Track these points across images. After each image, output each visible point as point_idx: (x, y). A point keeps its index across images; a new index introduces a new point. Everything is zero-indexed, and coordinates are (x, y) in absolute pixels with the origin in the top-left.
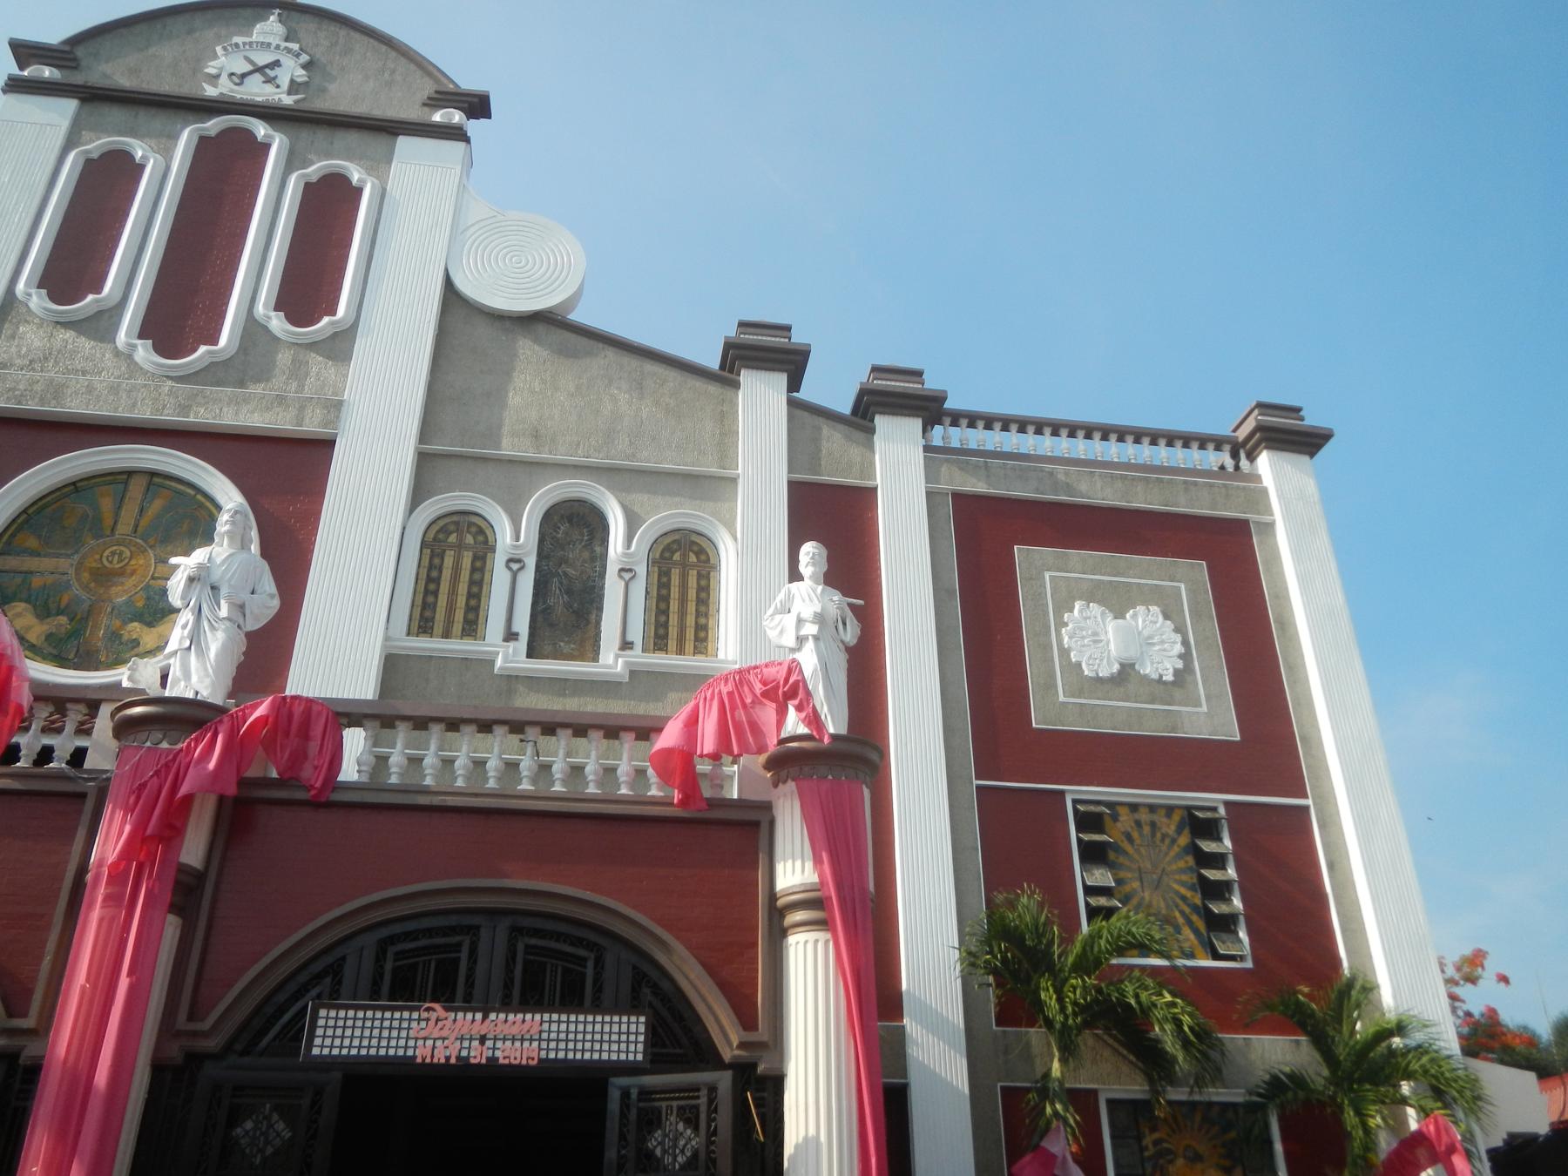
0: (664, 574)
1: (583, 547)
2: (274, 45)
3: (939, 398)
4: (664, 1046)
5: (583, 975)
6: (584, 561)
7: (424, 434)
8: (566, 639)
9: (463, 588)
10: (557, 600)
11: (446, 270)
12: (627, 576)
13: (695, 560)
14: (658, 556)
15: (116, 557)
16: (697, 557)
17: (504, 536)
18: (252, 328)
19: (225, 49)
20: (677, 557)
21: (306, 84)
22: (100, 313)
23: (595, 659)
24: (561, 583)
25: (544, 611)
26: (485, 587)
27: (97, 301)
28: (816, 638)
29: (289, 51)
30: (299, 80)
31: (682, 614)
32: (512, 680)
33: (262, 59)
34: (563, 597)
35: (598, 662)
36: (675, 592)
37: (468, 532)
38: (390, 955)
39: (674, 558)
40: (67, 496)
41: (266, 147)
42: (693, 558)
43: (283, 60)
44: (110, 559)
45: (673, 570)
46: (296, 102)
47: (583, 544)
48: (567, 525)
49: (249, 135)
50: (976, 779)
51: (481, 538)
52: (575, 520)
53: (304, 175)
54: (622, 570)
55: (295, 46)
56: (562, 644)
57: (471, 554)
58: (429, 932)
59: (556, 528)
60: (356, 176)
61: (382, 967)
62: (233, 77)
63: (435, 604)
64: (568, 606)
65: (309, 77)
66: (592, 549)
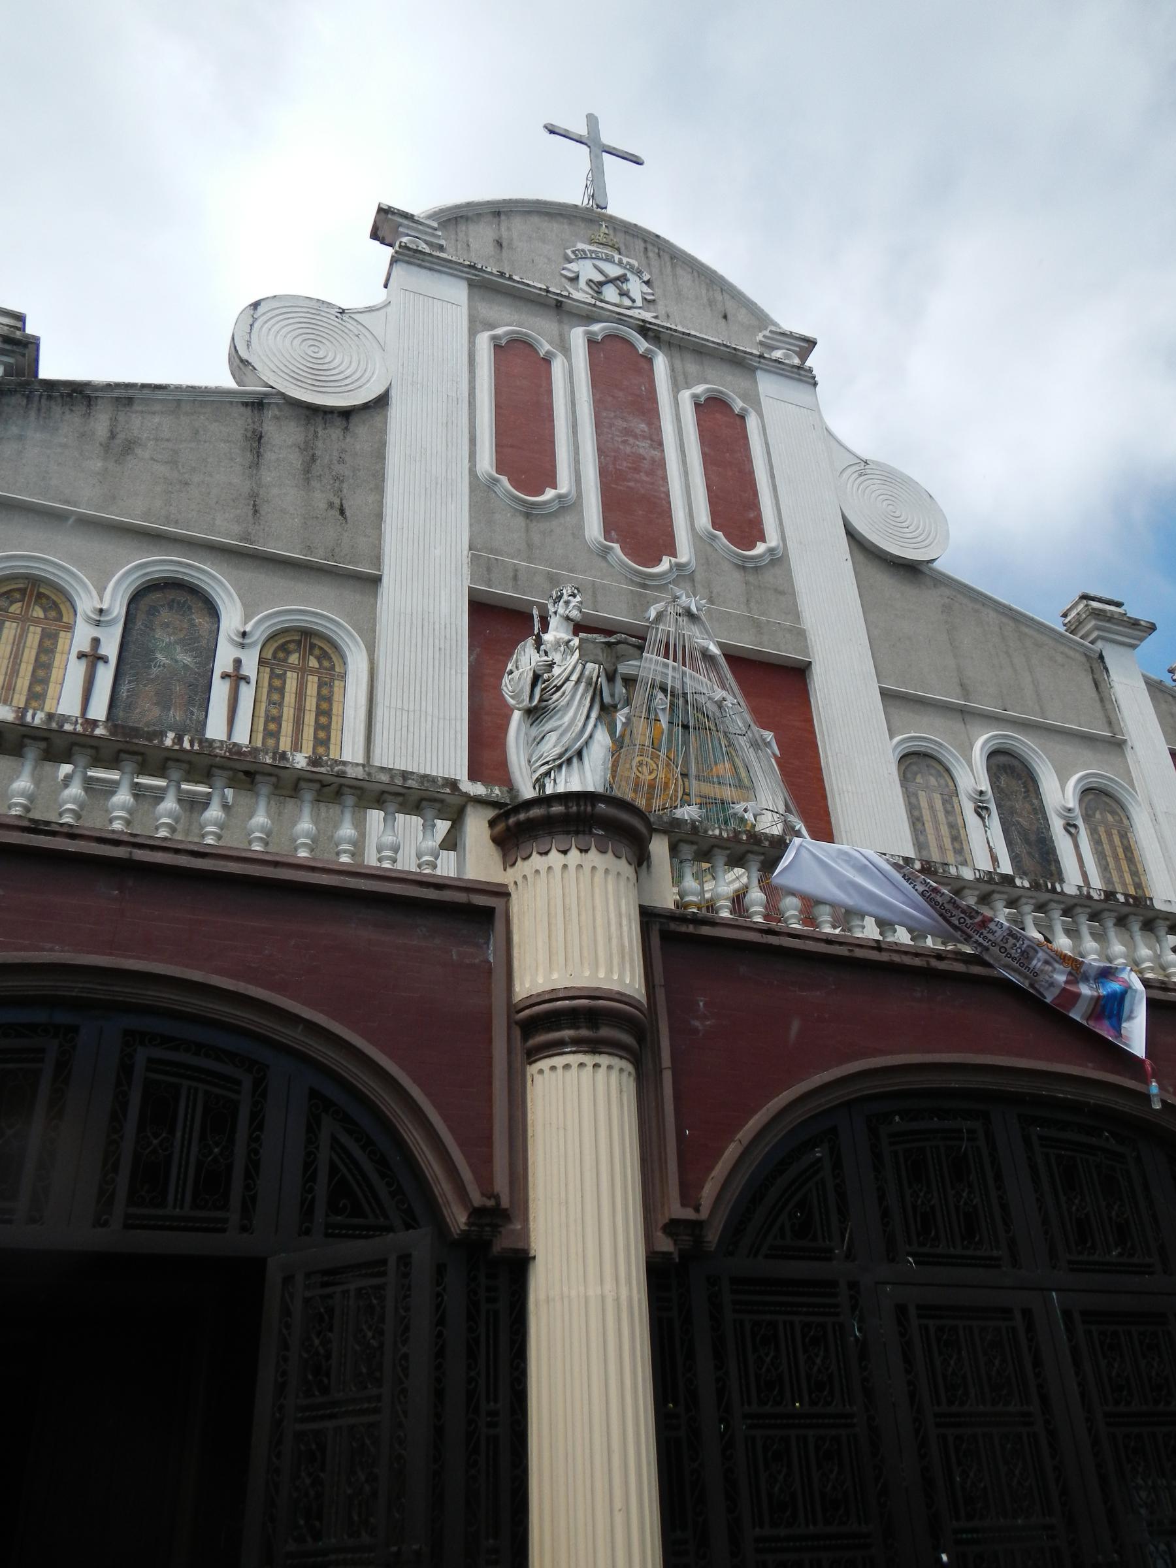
1: (1025, 798)
2: (616, 261)
9: (944, 830)
10: (1022, 849)
13: (1112, 820)
15: (645, 767)
19: (574, 252)
24: (1018, 832)
26: (962, 832)
30: (649, 297)
33: (614, 271)
36: (1106, 847)
37: (931, 775)
41: (649, 360)
43: (629, 275)
45: (1099, 828)
47: (1023, 794)
51: (942, 782)
54: (1068, 824)
59: (998, 778)
62: (591, 284)
64: (1029, 854)
66: (1030, 801)
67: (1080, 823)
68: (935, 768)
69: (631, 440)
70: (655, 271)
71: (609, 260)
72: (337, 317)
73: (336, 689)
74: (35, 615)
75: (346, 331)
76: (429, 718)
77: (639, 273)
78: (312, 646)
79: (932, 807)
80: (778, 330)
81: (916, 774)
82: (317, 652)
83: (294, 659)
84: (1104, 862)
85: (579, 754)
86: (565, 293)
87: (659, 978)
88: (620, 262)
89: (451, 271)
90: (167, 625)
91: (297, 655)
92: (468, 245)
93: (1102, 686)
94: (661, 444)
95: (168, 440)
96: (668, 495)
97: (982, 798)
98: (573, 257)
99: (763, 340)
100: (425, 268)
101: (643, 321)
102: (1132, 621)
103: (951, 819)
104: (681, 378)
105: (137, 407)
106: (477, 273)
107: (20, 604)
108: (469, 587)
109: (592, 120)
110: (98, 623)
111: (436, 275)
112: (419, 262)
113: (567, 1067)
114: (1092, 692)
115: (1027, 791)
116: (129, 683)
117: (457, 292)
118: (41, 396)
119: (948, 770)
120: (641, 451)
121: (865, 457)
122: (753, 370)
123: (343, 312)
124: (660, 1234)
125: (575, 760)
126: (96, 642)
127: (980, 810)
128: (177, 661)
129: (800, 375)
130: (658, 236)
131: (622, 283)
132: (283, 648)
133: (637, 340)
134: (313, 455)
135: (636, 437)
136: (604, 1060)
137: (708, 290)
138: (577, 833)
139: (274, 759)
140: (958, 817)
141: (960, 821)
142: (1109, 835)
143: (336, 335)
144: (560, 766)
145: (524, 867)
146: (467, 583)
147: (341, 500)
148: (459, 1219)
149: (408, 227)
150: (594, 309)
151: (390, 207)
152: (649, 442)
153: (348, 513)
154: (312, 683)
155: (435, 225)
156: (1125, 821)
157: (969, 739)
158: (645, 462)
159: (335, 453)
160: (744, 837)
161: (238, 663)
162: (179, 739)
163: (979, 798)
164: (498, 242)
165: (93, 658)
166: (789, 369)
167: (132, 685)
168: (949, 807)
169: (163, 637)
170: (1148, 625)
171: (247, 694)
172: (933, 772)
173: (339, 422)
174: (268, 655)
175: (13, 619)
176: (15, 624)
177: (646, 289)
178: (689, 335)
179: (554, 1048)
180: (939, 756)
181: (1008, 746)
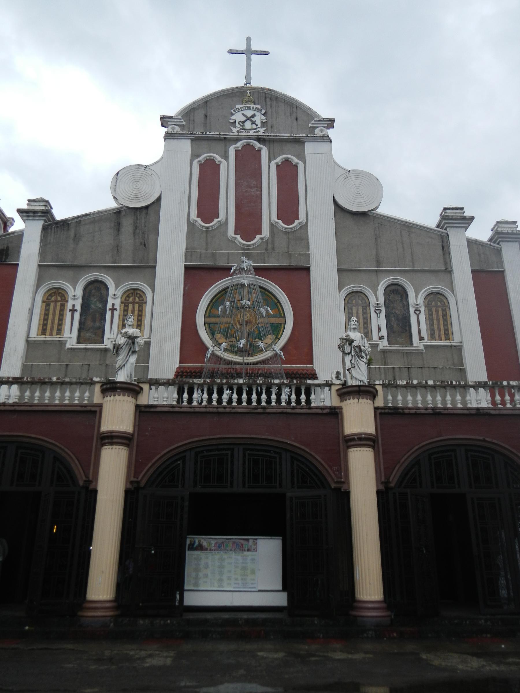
1: (400, 302)
2: (251, 109)
8: (400, 337)
10: (394, 323)
12: (418, 312)
13: (440, 304)
14: (426, 304)
16: (441, 303)
17: (372, 300)
18: (272, 226)
19: (234, 110)
20: (433, 303)
21: (266, 121)
22: (220, 226)
23: (411, 344)
24: (394, 316)
25: (390, 327)
26: (369, 320)
27: (219, 221)
29: (257, 109)
30: (264, 121)
31: (439, 325)
32: (384, 352)
33: (249, 113)
36: (435, 317)
37: (359, 299)
39: (433, 304)
40: (223, 294)
41: (259, 151)
42: (439, 304)
45: (433, 309)
46: (264, 131)
47: (399, 301)
48: (393, 294)
49: (252, 147)
53: (277, 163)
54: (416, 310)
55: (259, 107)
56: (399, 339)
57: (361, 307)
59: (389, 296)
60: (295, 160)
62: (240, 123)
64: (398, 324)
65: (266, 119)
68: (362, 297)
70: (269, 107)
71: (249, 109)
72: (144, 170)
73: (144, 307)
74: (58, 299)
75: (147, 174)
76: (169, 314)
77: (260, 111)
78: (137, 294)
80: (319, 119)
81: (353, 300)
82: (138, 295)
83: (131, 299)
85: (124, 365)
86: (227, 134)
87: (137, 424)
88: (253, 107)
90: (94, 295)
91: (132, 298)
92: (194, 121)
93: (446, 248)
94: (261, 188)
95: (91, 233)
97: (378, 306)
98: (234, 112)
99: (312, 125)
100: (175, 139)
101: (258, 136)
102: (462, 217)
103: (365, 316)
104: (272, 155)
105: (82, 223)
106: (193, 135)
107: (54, 297)
108: (184, 264)
109: (249, 40)
110: (74, 299)
111: (179, 140)
112: (173, 137)
113: (109, 448)
114: (440, 252)
115: (402, 299)
116: (84, 316)
117: (186, 145)
118: (55, 227)
119: (367, 297)
122: (303, 143)
123: (146, 167)
124: (129, 484)
125: (123, 368)
126: (74, 306)
127: (377, 311)
128: (97, 307)
129: (324, 139)
130: (270, 90)
131: (253, 118)
132: (128, 296)
134: (136, 226)
135: (251, 188)
136: (114, 447)
137: (290, 108)
138: (113, 391)
139: (48, 380)
140: (368, 314)
142: (437, 311)
143: (144, 178)
144: (119, 370)
145: (106, 399)
146: (183, 263)
147: (145, 241)
148: (81, 483)
149: (171, 121)
150: (238, 136)
151: (164, 116)
152: (256, 188)
153: (147, 246)
154: (137, 306)
155: (180, 117)
156: (446, 304)
157: (378, 283)
159: (143, 224)
160: (171, 381)
161: (113, 305)
162: (27, 378)
163: (377, 306)
164: (205, 115)
165: (73, 311)
166: (319, 138)
167: (84, 317)
168: (365, 311)
169: (94, 299)
170: (471, 217)
171: (116, 314)
172: (360, 298)
173: (144, 211)
174: (123, 299)
175: (53, 302)
176: (53, 304)
177: (263, 117)
178: (276, 136)
179: (103, 445)
180: (364, 292)
181: (396, 282)
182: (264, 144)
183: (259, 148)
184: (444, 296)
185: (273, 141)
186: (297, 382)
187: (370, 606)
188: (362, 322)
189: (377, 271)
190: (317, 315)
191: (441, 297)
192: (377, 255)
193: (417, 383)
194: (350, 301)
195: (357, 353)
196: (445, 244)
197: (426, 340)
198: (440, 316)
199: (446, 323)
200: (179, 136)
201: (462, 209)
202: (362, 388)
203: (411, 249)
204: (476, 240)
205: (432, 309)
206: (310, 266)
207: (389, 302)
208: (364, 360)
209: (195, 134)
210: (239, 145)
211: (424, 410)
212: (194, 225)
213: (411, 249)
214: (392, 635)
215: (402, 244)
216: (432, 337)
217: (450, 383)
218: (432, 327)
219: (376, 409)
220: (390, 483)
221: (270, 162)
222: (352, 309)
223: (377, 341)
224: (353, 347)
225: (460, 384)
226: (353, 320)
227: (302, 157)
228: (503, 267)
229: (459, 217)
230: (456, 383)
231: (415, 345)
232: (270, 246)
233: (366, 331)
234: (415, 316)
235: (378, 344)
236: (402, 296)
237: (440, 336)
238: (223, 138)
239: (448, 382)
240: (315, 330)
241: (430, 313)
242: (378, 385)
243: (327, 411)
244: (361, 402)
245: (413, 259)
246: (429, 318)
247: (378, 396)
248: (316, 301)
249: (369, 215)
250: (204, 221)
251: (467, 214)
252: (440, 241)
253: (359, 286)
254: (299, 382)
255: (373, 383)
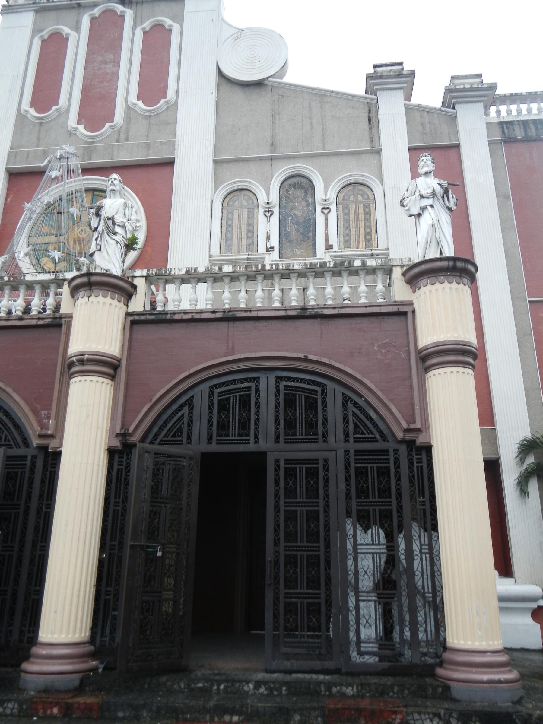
0: (346, 208)
1: (303, 199)
3: (493, 87)
4: (363, 433)
5: (316, 399)
6: (303, 207)
7: (216, 151)
9: (245, 228)
10: (291, 228)
11: (218, 65)
12: (326, 211)
13: (361, 199)
14: (341, 199)
18: (129, 109)
20: (352, 198)
22: (59, 115)
24: (292, 219)
25: (286, 234)
26: (255, 227)
28: (432, 206)
31: (357, 227)
34: (294, 227)
35: (316, 256)
36: (352, 216)
38: (216, 395)
39: (350, 199)
41: (122, 17)
42: (360, 198)
44: (81, 233)
45: (350, 206)
48: (293, 189)
49: (113, 12)
50: (528, 298)
52: (297, 186)
53: (144, 28)
54: (324, 208)
56: (297, 250)
57: (246, 210)
58: (235, 382)
59: (287, 191)
60: (168, 22)
61: (212, 400)
63: (232, 237)
64: (297, 231)
67: (333, 208)
69: (103, 66)
79: (240, 218)
84: (347, 225)
89: (26, 9)
93: (374, 120)
94: (119, 63)
96: (116, 89)
97: (269, 206)
102: (397, 74)
103: (250, 221)
104: (139, 20)
111: (19, 14)
114: (366, 125)
115: (306, 195)
119: (255, 195)
120: (108, 71)
121: (241, 28)
133: (117, 8)
141: (255, 221)
142: (356, 208)
146: (5, 166)
152: (113, 64)
156: (371, 197)
157: (272, 174)
158: (108, 75)
163: (267, 206)
168: (251, 215)
170: (409, 72)
172: (246, 197)
182: (130, 6)
183: (122, 12)
184: (368, 187)
185: (143, 2)
186: (9, 279)
187: (44, 652)
188: (246, 230)
189: (272, 159)
190: (177, 222)
191: (363, 189)
192: (273, 137)
193: (205, 271)
194: (231, 203)
195: (108, 227)
196: (373, 115)
197: (335, 248)
198: (360, 215)
199: (368, 224)
200: (19, 8)
201: (401, 64)
202: (93, 279)
203: (323, 125)
204: (419, 105)
205: (348, 205)
206: (174, 158)
207: (286, 200)
208: (118, 238)
209: (39, 3)
210: (97, 11)
211: (210, 314)
212: (25, 117)
213: (323, 125)
214: (49, 712)
215: (311, 119)
216: (347, 244)
217: (260, 268)
218: (347, 231)
219: (128, 314)
220: (130, 435)
221: (136, 29)
222: (232, 213)
223: (263, 254)
224: (105, 219)
225: (277, 269)
226: (112, 179)
227: (179, 18)
228: (457, 138)
229: (392, 73)
230: (272, 267)
231: (318, 256)
232: (123, 136)
233: (250, 241)
234: (323, 216)
235: (264, 259)
236: (306, 191)
237: (358, 243)
238: (76, 6)
239: (257, 267)
240: (173, 243)
241: (346, 211)
242: (139, 278)
243: (49, 321)
244: (92, 302)
245: (324, 138)
246: (344, 218)
247: (136, 294)
248: (178, 204)
249: (266, 85)
250: (38, 111)
251: (407, 68)
252: (367, 111)
253: (244, 181)
254: (12, 279)
255: (131, 275)
